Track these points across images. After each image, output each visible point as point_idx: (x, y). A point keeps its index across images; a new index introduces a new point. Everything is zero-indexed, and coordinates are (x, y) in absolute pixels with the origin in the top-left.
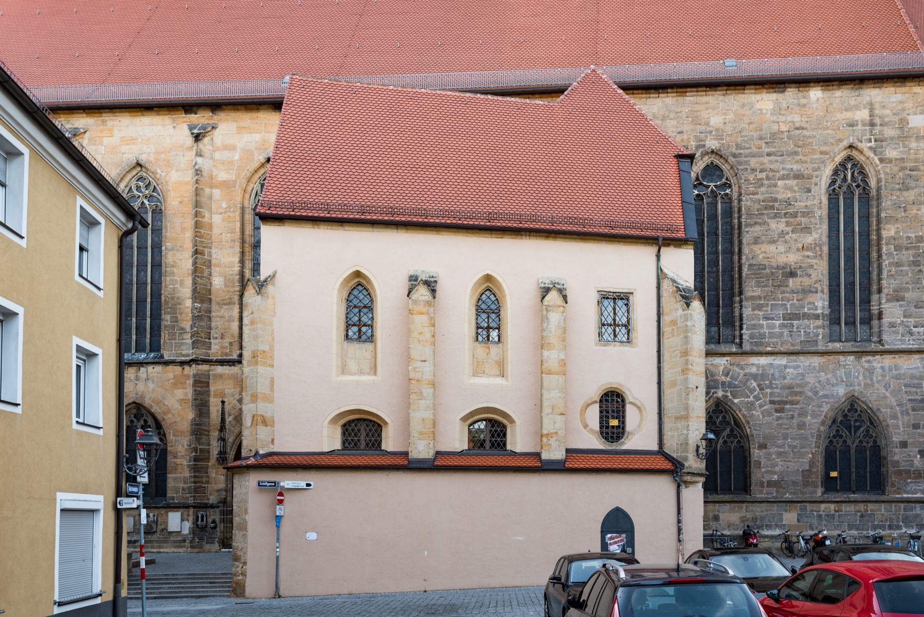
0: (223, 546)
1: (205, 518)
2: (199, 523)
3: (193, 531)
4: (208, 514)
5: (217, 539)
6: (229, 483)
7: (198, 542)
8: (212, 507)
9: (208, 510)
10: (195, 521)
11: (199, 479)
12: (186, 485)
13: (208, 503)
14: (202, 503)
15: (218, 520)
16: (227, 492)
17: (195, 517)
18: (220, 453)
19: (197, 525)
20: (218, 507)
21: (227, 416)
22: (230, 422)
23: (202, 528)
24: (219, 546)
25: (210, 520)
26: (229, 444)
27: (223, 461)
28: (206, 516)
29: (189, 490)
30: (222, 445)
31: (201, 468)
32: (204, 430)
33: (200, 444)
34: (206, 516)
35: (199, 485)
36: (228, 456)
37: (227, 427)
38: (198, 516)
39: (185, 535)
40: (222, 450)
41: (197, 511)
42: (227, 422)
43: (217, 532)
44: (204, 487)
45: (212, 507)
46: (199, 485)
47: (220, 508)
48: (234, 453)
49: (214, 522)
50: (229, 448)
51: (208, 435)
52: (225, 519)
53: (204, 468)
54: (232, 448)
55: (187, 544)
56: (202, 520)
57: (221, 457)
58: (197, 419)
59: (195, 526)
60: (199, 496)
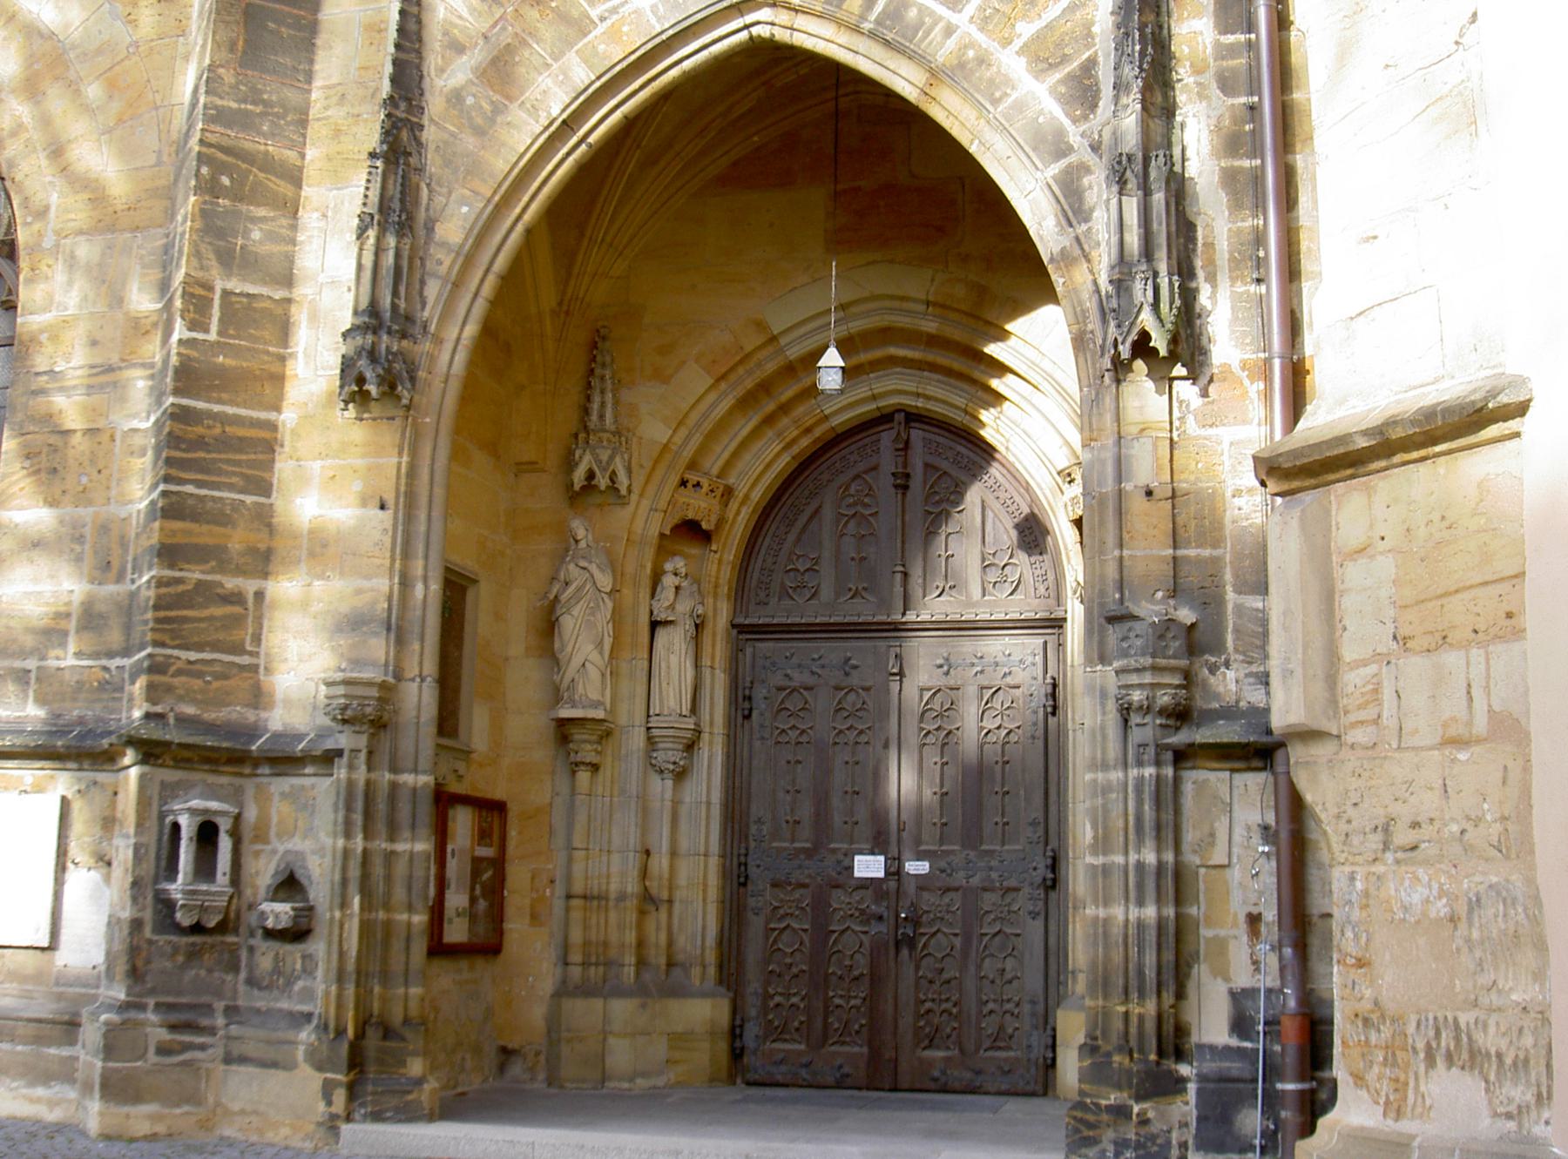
0: (353, 1091)
1: (225, 844)
2: (176, 888)
3: (133, 951)
4: (251, 814)
5: (306, 1035)
6: (418, 567)
7: (163, 1050)
8: (284, 760)
9: (249, 786)
10: (149, 867)
11: (203, 534)
12: (111, 588)
13: (253, 732)
14: (211, 728)
15: (320, 875)
16: (400, 642)
17: (151, 838)
18: (371, 320)
19: (165, 905)
20: (328, 758)
21: (433, 59)
22: (456, 97)
23: (197, 929)
24: (327, 1091)
25: (263, 871)
26: (442, 261)
27: (390, 385)
28: (236, 835)
29: (128, 628)
30: (389, 259)
31: (225, 443)
32: (268, 164)
33: (227, 259)
34: (236, 835)
35: (194, 574)
36: (427, 346)
37: (429, 135)
38: (176, 827)
39: (79, 981)
40: (386, 301)
41: (169, 791)
42: (435, 104)
43: (308, 971)
44: (236, 598)
45: (284, 760)
46: (194, 574)
47: (341, 773)
48: (471, 330)
49: (289, 885)
50: (432, 290)
51: (292, 209)
52: (378, 870)
53: (242, 444)
54: (457, 285)
55: (87, 1054)
56: (205, 866)
57: (373, 355)
58: (228, 76)
59: (148, 915)
60: (191, 670)
